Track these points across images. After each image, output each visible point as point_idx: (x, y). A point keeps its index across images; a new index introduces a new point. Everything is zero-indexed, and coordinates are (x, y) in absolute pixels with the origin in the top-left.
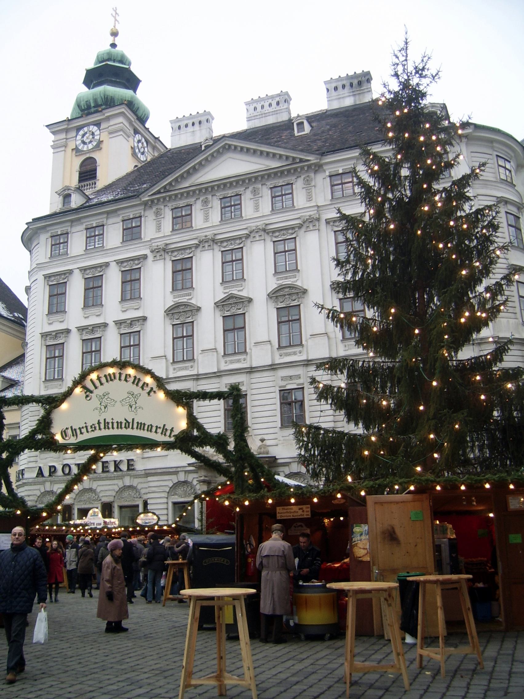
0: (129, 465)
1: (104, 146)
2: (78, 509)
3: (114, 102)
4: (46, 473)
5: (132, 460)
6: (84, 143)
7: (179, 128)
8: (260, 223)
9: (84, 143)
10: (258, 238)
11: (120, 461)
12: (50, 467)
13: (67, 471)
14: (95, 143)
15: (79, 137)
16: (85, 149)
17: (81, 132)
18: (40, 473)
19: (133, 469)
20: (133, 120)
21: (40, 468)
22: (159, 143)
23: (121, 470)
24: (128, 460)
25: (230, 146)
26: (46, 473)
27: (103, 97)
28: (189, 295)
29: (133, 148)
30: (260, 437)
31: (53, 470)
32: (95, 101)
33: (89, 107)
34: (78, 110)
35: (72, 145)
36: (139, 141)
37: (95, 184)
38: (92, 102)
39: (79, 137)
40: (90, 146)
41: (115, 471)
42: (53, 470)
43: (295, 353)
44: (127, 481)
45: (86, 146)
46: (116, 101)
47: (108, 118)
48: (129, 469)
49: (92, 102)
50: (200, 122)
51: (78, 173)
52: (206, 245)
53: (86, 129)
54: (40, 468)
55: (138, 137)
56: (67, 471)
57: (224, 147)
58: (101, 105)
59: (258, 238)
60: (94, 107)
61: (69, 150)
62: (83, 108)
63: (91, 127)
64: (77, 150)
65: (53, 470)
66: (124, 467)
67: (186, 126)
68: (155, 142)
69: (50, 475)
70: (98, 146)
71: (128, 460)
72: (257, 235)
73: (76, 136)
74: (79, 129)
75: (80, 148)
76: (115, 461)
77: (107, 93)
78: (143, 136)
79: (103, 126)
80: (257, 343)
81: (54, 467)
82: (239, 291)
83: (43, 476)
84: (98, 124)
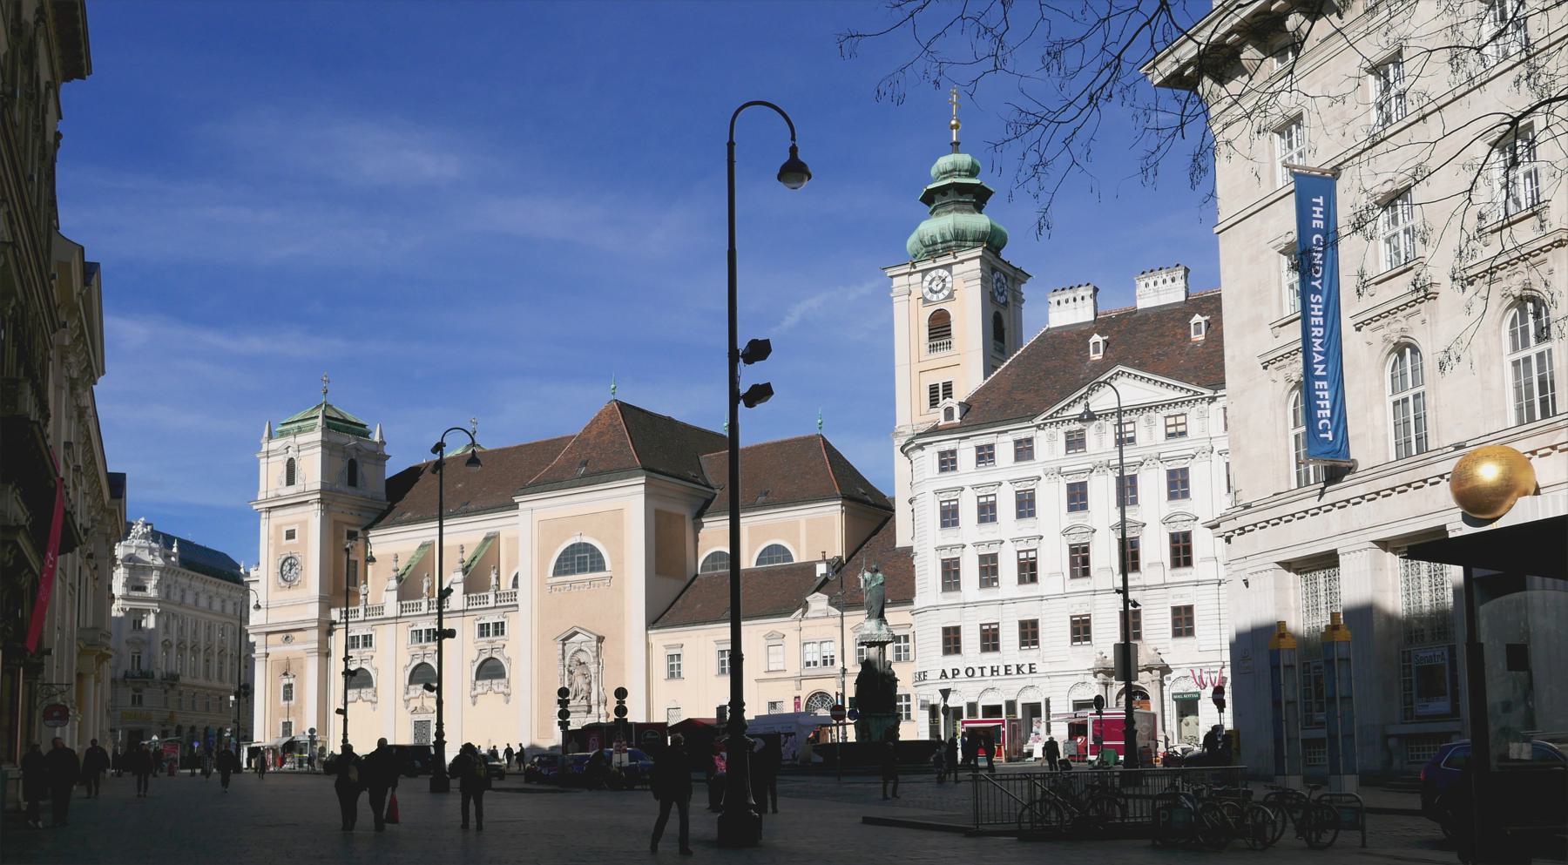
0: (1031, 668)
1: (956, 295)
2: (983, 706)
3: (966, 236)
4: (950, 674)
6: (931, 290)
7: (1059, 303)
8: (1154, 452)
9: (931, 290)
10: (1151, 466)
13: (970, 672)
14: (946, 292)
15: (926, 284)
16: (935, 298)
17: (928, 278)
18: (944, 674)
19: (1035, 672)
20: (991, 259)
21: (944, 671)
22: (1020, 273)
23: (1023, 673)
24: (1030, 665)
25: (1123, 372)
26: (950, 674)
28: (1085, 517)
29: (992, 293)
30: (1153, 647)
31: (956, 672)
32: (943, 236)
33: (935, 243)
34: (920, 245)
35: (917, 292)
36: (998, 280)
37: (950, 343)
38: (938, 236)
39: (926, 284)
40: (941, 296)
41: (1018, 673)
43: (1186, 574)
44: (1028, 682)
45: (935, 296)
46: (968, 235)
47: (962, 262)
48: (1031, 672)
49: (938, 236)
50: (1083, 298)
51: (927, 328)
52: (1101, 470)
53: (933, 273)
54: (944, 671)
55: (997, 275)
56: (970, 672)
57: (1117, 374)
58: (951, 241)
59: (1151, 466)
60: (941, 243)
61: (913, 298)
62: (927, 243)
63: (941, 271)
64: (926, 301)
65: (956, 672)
66: (1026, 669)
67: (1067, 301)
68: (1015, 274)
69: (953, 677)
70: (950, 297)
71: (1030, 665)
72: (1151, 463)
73: (922, 282)
74: (925, 272)
75: (928, 297)
76: (1017, 665)
77: (957, 227)
78: (1001, 272)
79: (956, 269)
80: (1150, 565)
82: (1134, 515)
83: (947, 677)
84: (948, 267)
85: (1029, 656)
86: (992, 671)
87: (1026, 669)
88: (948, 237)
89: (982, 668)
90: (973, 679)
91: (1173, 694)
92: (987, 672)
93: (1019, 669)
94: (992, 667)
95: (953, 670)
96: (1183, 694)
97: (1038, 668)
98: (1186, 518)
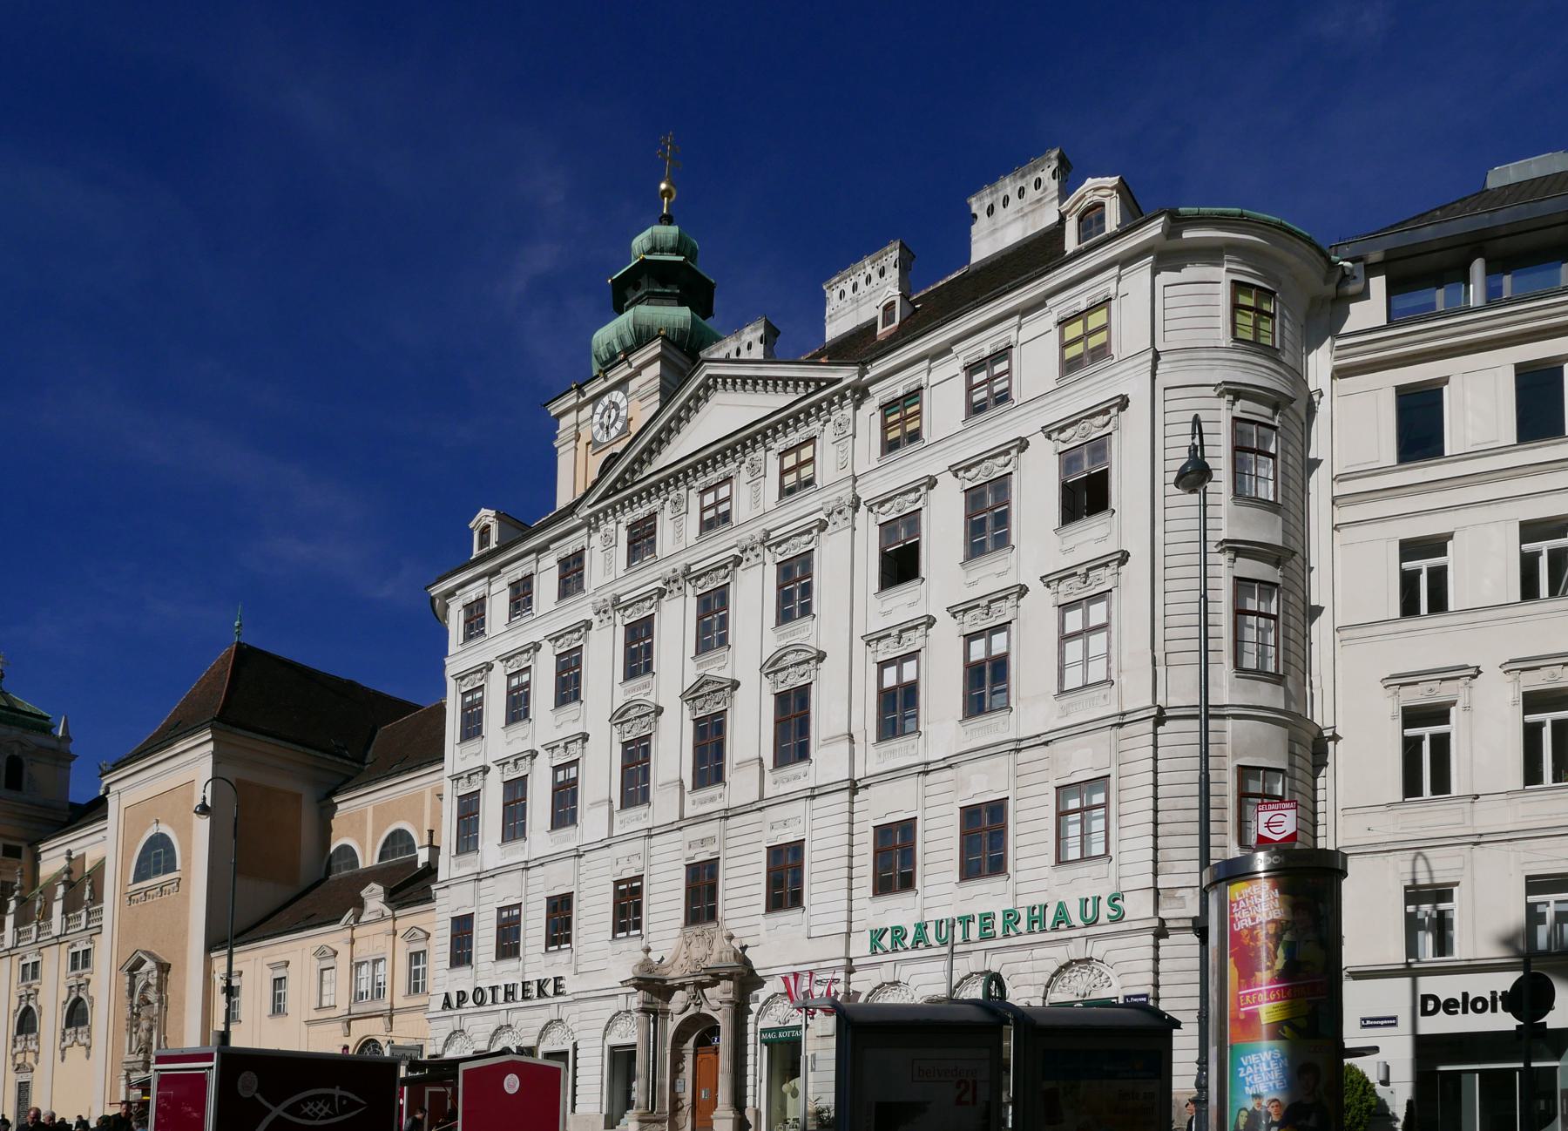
0: (556, 986)
5: (561, 978)
11: (545, 980)
12: (458, 992)
19: (561, 994)
24: (556, 979)
27: (632, 330)
32: (621, 340)
38: (616, 342)
42: (462, 996)
48: (556, 993)
54: (447, 994)
66: (550, 989)
71: (556, 979)
76: (539, 981)
81: (463, 992)
83: (450, 1007)
85: (556, 964)
86: (506, 993)
87: (550, 989)
88: (629, 341)
89: (494, 989)
90: (482, 1009)
91: (764, 1031)
92: (501, 994)
93: (541, 985)
94: (506, 986)
95: (458, 992)
96: (777, 1030)
97: (569, 986)
98: (803, 656)
